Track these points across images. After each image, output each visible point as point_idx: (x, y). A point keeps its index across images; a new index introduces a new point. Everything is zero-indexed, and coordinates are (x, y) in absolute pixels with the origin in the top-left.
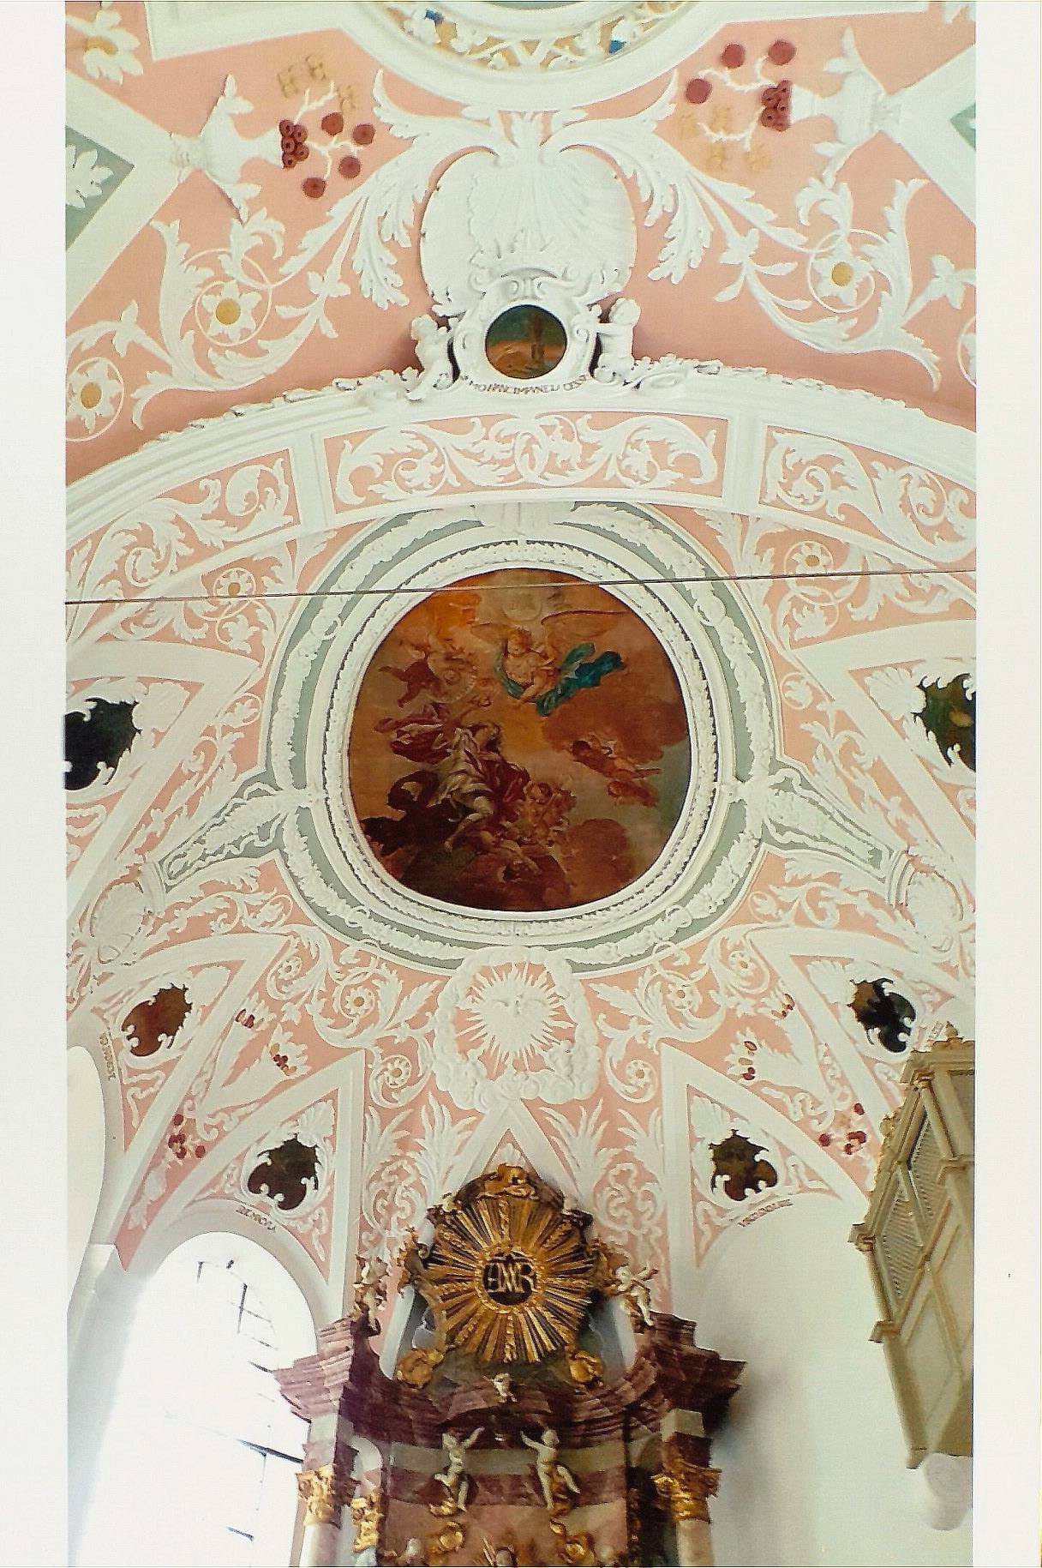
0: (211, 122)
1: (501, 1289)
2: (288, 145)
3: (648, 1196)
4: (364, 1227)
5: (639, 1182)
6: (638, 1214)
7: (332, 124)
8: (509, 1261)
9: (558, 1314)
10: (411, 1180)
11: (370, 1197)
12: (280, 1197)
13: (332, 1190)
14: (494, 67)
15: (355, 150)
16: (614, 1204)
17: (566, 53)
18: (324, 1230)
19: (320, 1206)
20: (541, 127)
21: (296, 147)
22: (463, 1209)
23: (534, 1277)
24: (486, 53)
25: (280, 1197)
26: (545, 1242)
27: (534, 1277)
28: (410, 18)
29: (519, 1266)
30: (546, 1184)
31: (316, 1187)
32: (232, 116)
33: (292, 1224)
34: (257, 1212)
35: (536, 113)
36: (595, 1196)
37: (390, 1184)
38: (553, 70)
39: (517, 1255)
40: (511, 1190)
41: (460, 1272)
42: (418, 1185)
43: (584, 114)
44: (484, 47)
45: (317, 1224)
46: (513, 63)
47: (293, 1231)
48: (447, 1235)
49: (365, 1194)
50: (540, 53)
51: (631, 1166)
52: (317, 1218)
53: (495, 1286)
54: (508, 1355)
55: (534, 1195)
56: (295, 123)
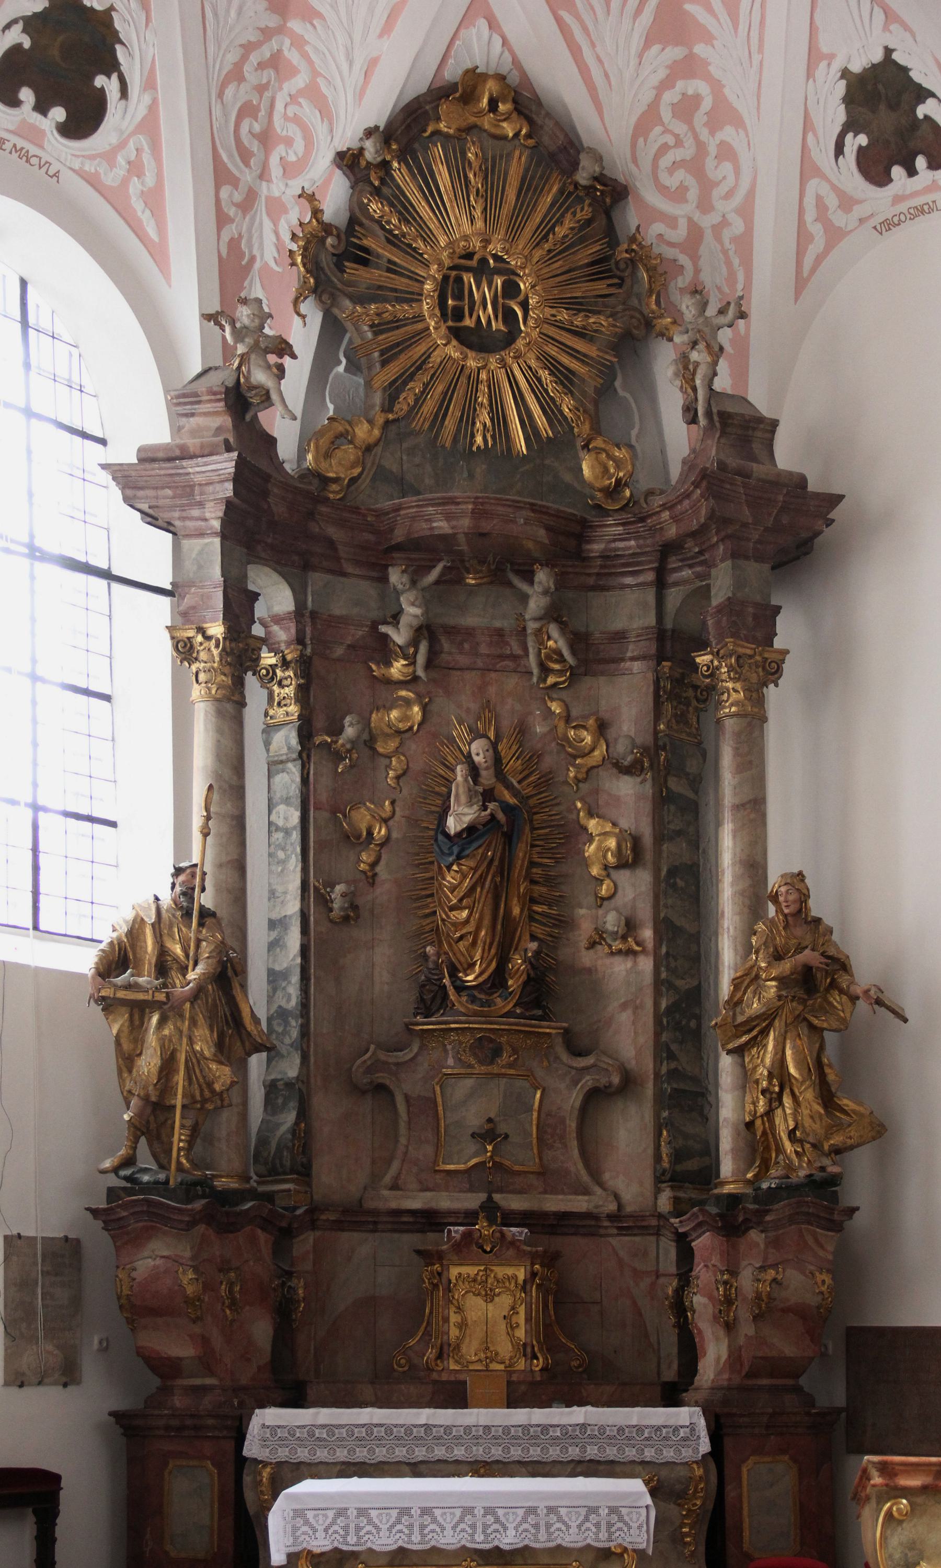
1: (468, 322)
3: (727, 153)
4: (222, 176)
5: (714, 125)
6: (707, 186)
8: (482, 271)
9: (565, 378)
10: (300, 81)
11: (226, 115)
12: (58, 114)
13: (155, 101)
16: (666, 161)
18: (150, 180)
19: (134, 133)
22: (402, 159)
23: (525, 305)
25: (58, 114)
26: (546, 238)
27: (525, 305)
29: (499, 282)
30: (548, 115)
31: (124, 92)
33: (89, 167)
34: (21, 143)
36: (634, 145)
37: (261, 89)
39: (496, 258)
40: (487, 122)
41: (401, 283)
42: (313, 93)
45: (135, 168)
47: (93, 181)
48: (375, 207)
49: (217, 111)
51: (699, 86)
52: (133, 157)
53: (458, 314)
54: (479, 440)
55: (529, 136)
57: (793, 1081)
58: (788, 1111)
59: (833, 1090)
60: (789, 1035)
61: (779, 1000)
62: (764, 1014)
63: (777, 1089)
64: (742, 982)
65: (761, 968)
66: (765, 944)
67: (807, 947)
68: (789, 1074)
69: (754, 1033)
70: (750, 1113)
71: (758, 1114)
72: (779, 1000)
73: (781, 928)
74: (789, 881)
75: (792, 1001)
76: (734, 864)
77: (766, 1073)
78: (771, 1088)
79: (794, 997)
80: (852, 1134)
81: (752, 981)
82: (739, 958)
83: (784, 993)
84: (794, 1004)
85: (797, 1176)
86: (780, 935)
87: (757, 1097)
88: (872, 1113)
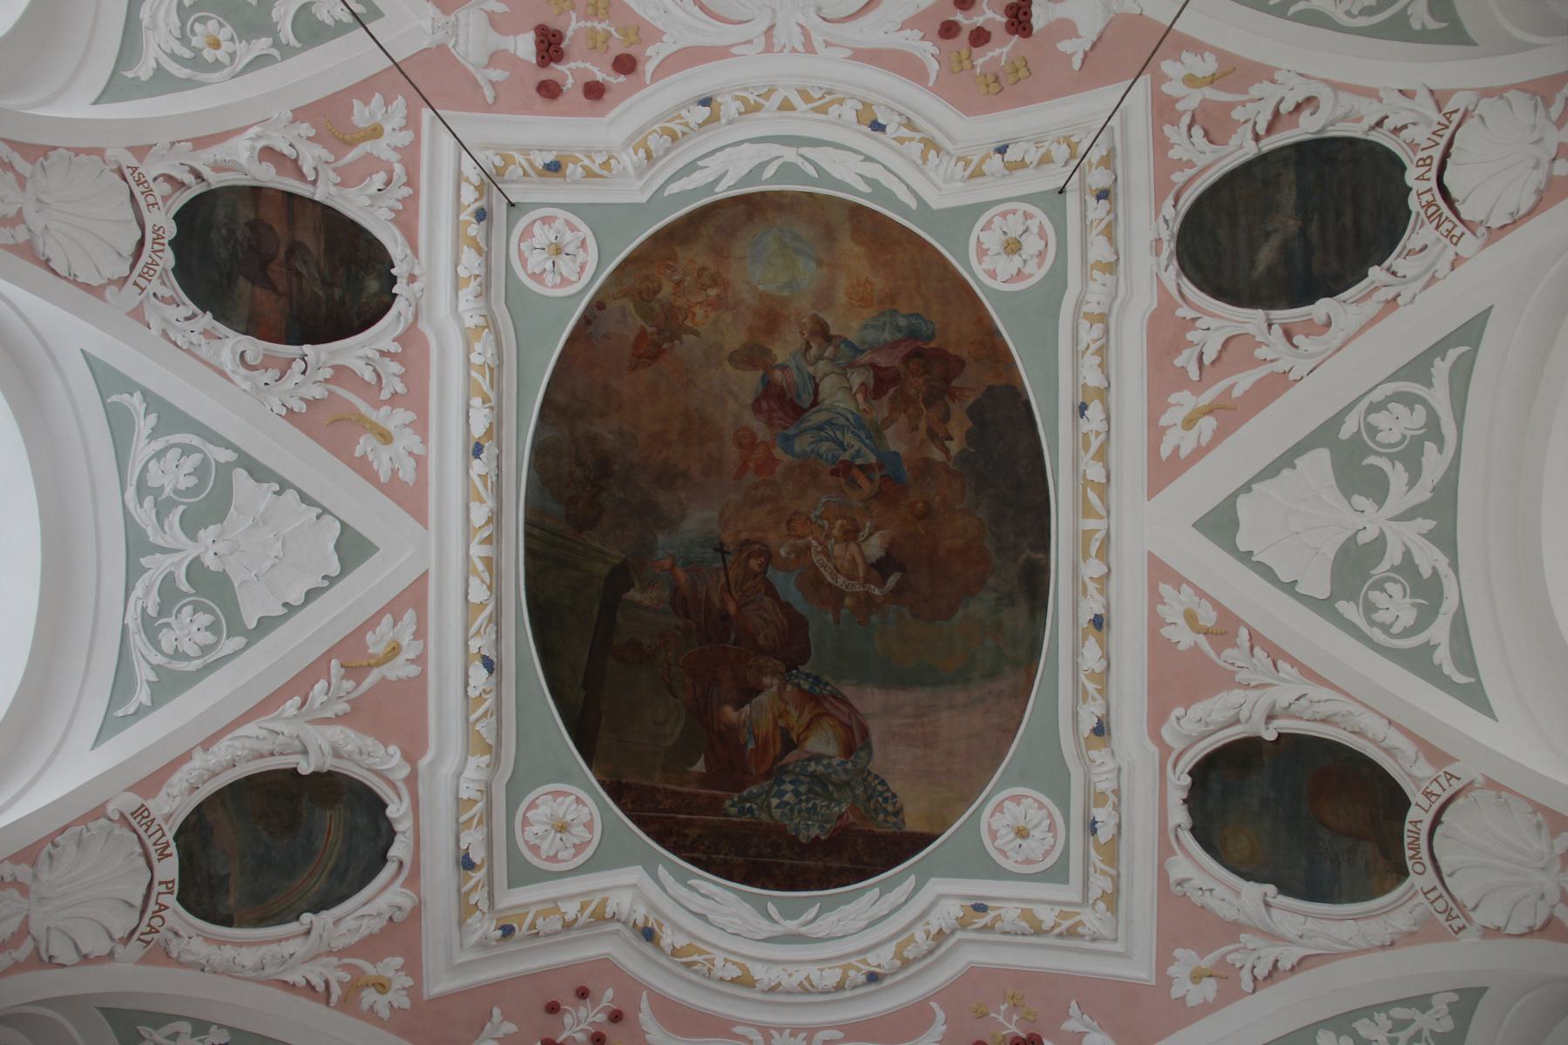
0: (1099, 27)
2: (1025, 14)
7: (980, 37)
14: (821, 89)
15: (959, 17)
17: (752, 98)
20: (775, 40)
21: (1017, 14)
24: (828, 98)
28: (900, 124)
32: (1079, 37)
35: (781, 51)
38: (764, 86)
43: (734, 51)
44: (832, 103)
46: (805, 95)
50: (776, 99)
56: (1017, 36)
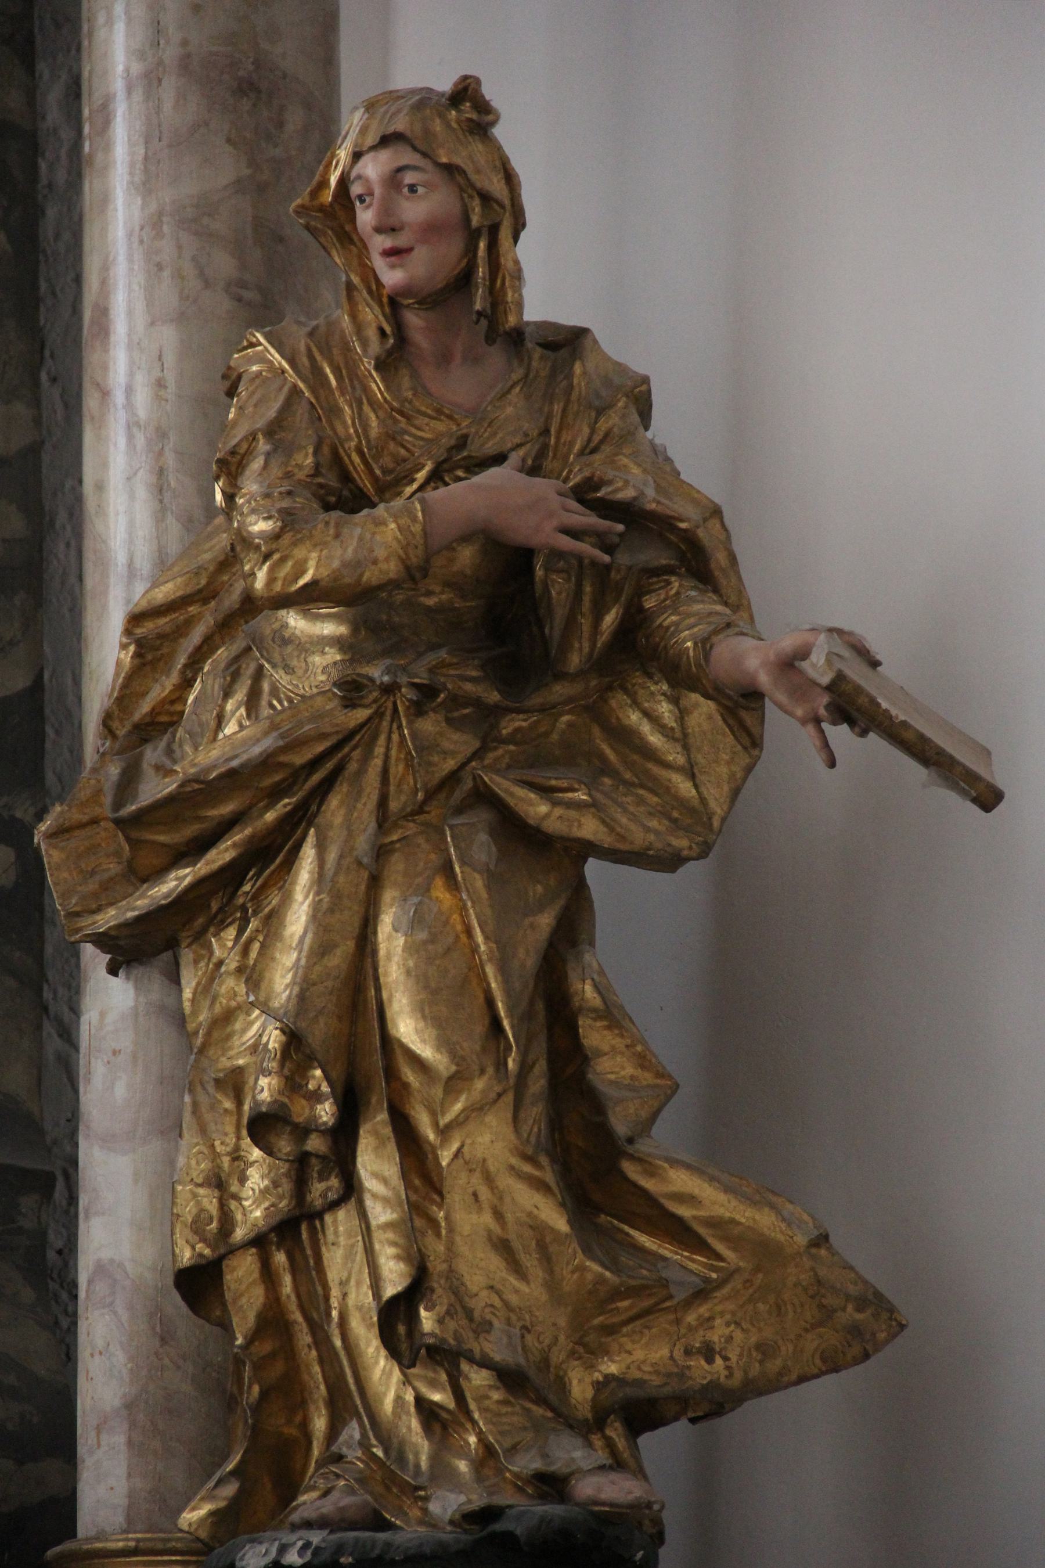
57: (410, 1076)
58: (380, 1214)
59: (620, 1127)
60: (397, 864)
61: (349, 704)
62: (266, 763)
63: (326, 1112)
64: (181, 630)
65: (243, 541)
66: (272, 431)
67: (499, 459)
68: (388, 1043)
69: (222, 854)
70: (197, 1227)
71: (240, 1234)
72: (349, 704)
73: (368, 364)
74: (400, 125)
75: (418, 709)
76: (152, 79)
77: (274, 1039)
78: (300, 1111)
79: (427, 692)
80: (716, 1336)
81: (225, 626)
82: (174, 527)
83: (377, 672)
84: (428, 725)
85: (427, 1520)
86: (361, 397)
87: (236, 1156)
88: (822, 1240)
